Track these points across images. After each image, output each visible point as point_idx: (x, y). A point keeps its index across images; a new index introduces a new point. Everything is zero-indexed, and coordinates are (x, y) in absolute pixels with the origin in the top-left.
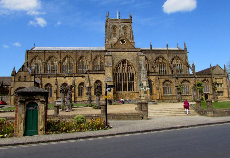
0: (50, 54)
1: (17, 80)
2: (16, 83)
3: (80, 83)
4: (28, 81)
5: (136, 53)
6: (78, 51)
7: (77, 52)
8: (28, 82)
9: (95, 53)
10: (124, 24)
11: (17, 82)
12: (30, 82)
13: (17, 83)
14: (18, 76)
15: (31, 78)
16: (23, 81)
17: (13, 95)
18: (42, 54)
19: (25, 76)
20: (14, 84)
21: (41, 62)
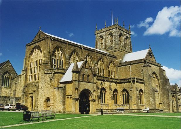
0: (73, 48)
1: (81, 79)
2: (80, 82)
3: (114, 89)
4: (91, 81)
5: (159, 68)
6: (97, 52)
7: (96, 52)
8: (91, 83)
9: (109, 57)
10: (126, 35)
11: (81, 81)
12: (93, 83)
13: (82, 82)
14: (82, 74)
15: (93, 79)
16: (86, 81)
17: (78, 99)
18: (65, 46)
19: (88, 76)
20: (79, 84)
21: (62, 56)
